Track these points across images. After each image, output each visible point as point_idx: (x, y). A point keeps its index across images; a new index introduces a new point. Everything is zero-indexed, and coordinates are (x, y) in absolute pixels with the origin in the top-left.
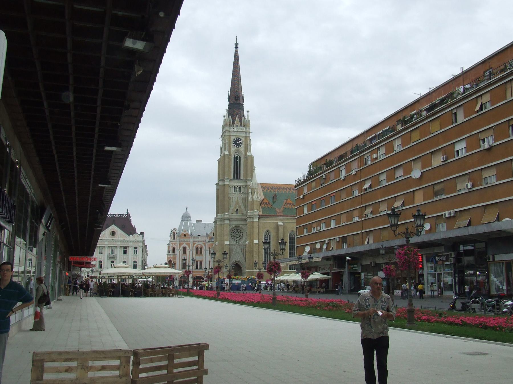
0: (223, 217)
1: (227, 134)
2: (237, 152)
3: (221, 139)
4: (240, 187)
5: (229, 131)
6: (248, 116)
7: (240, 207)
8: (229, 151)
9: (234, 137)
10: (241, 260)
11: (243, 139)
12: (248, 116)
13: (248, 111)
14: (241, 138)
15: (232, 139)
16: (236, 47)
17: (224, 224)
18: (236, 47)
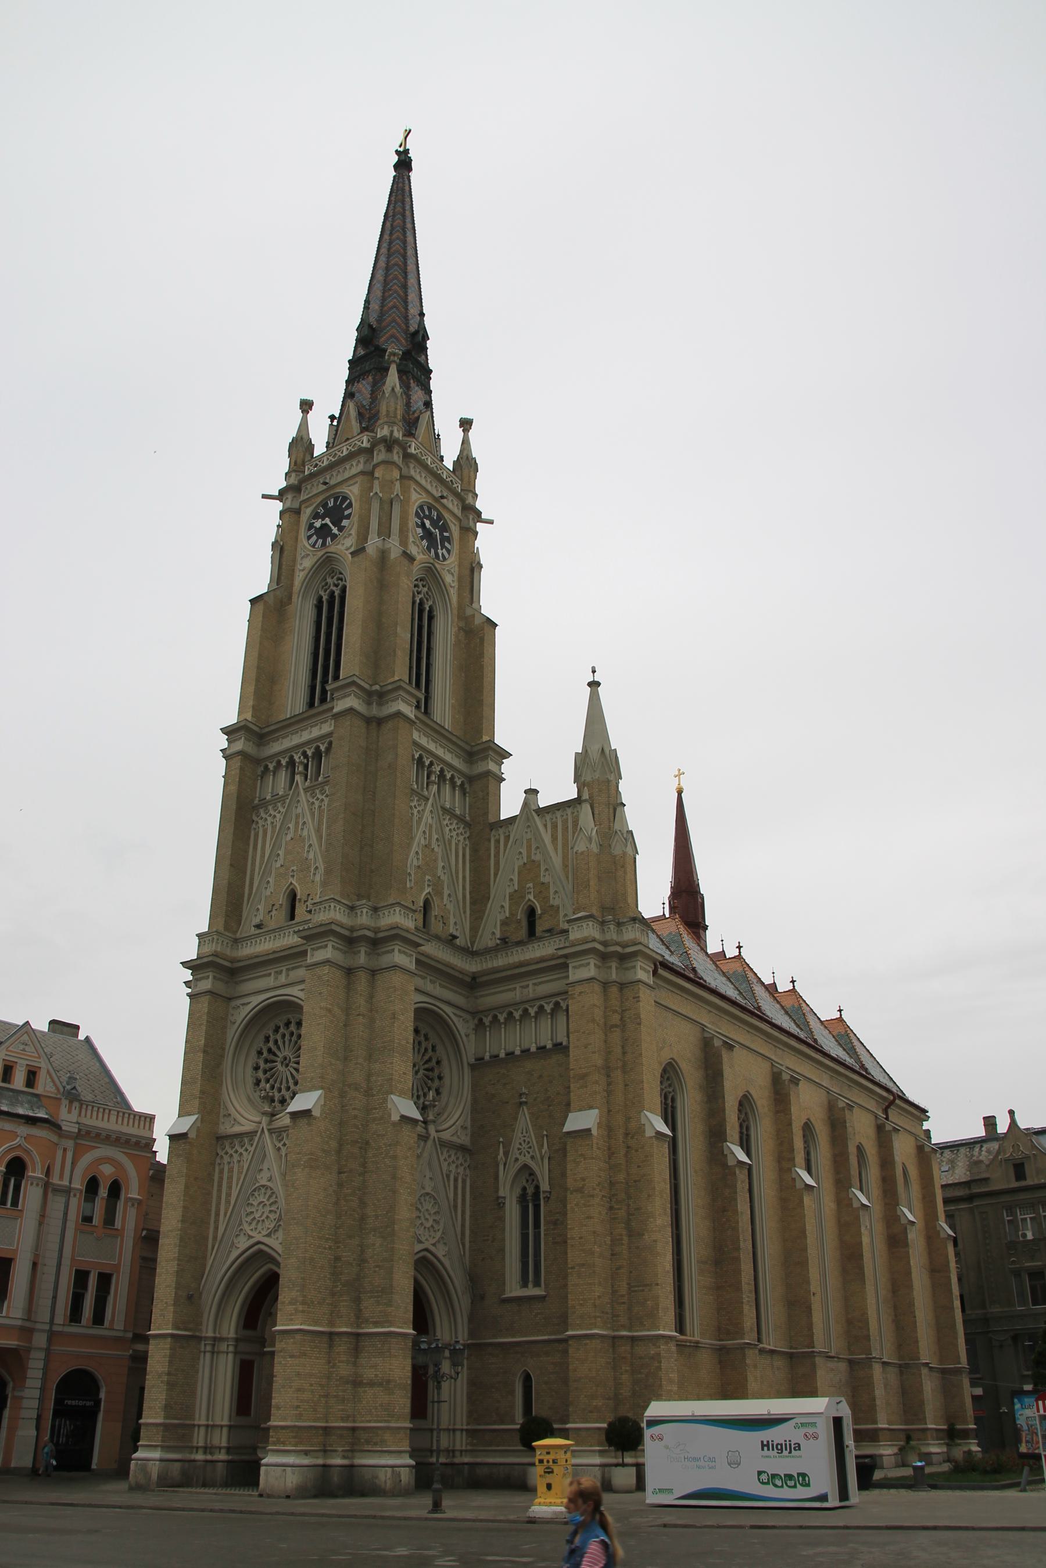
0: (364, 918)
1: (396, 457)
2: (430, 576)
3: (279, 506)
4: (442, 775)
5: (407, 456)
6: (465, 442)
7: (437, 886)
8: (404, 542)
9: (424, 498)
10: (440, 1252)
11: (455, 530)
12: (465, 442)
13: (466, 424)
14: (446, 515)
15: (417, 498)
16: (404, 164)
17: (373, 973)
18: (404, 164)
